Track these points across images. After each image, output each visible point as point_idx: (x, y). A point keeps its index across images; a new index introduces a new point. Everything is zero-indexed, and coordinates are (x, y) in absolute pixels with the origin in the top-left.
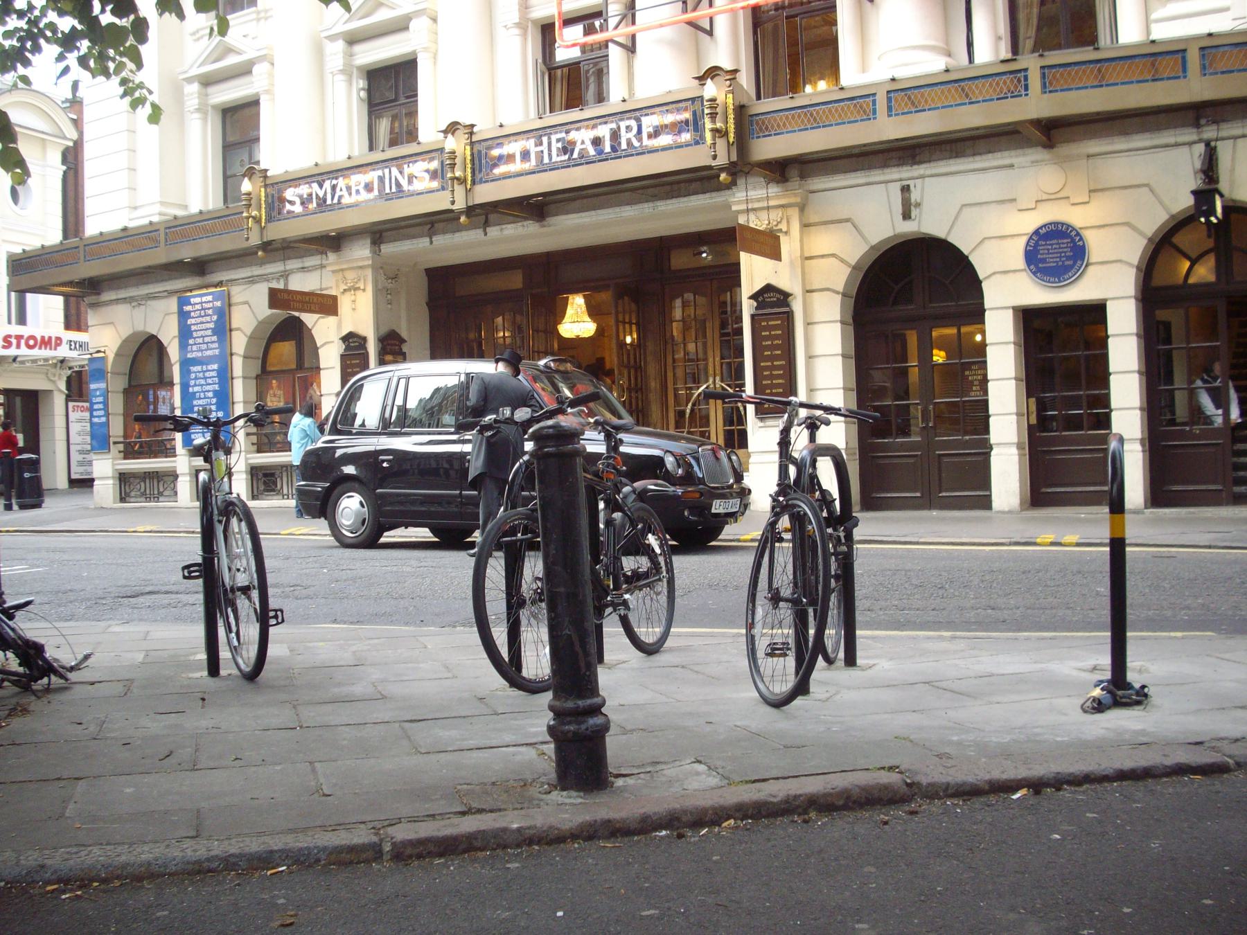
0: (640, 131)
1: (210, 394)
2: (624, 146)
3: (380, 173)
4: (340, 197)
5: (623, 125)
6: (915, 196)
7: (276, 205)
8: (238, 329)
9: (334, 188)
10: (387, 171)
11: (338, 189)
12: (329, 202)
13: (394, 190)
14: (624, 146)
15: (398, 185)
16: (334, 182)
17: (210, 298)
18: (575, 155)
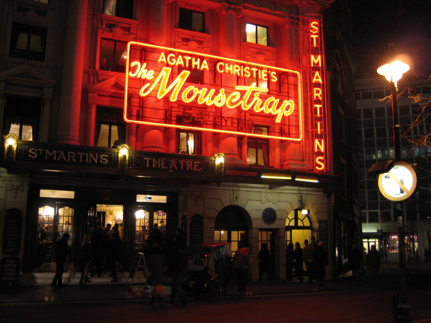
2: (188, 169)
3: (84, 154)
9: (58, 155)
11: (61, 155)
12: (55, 159)
13: (90, 162)
14: (188, 169)
16: (58, 152)
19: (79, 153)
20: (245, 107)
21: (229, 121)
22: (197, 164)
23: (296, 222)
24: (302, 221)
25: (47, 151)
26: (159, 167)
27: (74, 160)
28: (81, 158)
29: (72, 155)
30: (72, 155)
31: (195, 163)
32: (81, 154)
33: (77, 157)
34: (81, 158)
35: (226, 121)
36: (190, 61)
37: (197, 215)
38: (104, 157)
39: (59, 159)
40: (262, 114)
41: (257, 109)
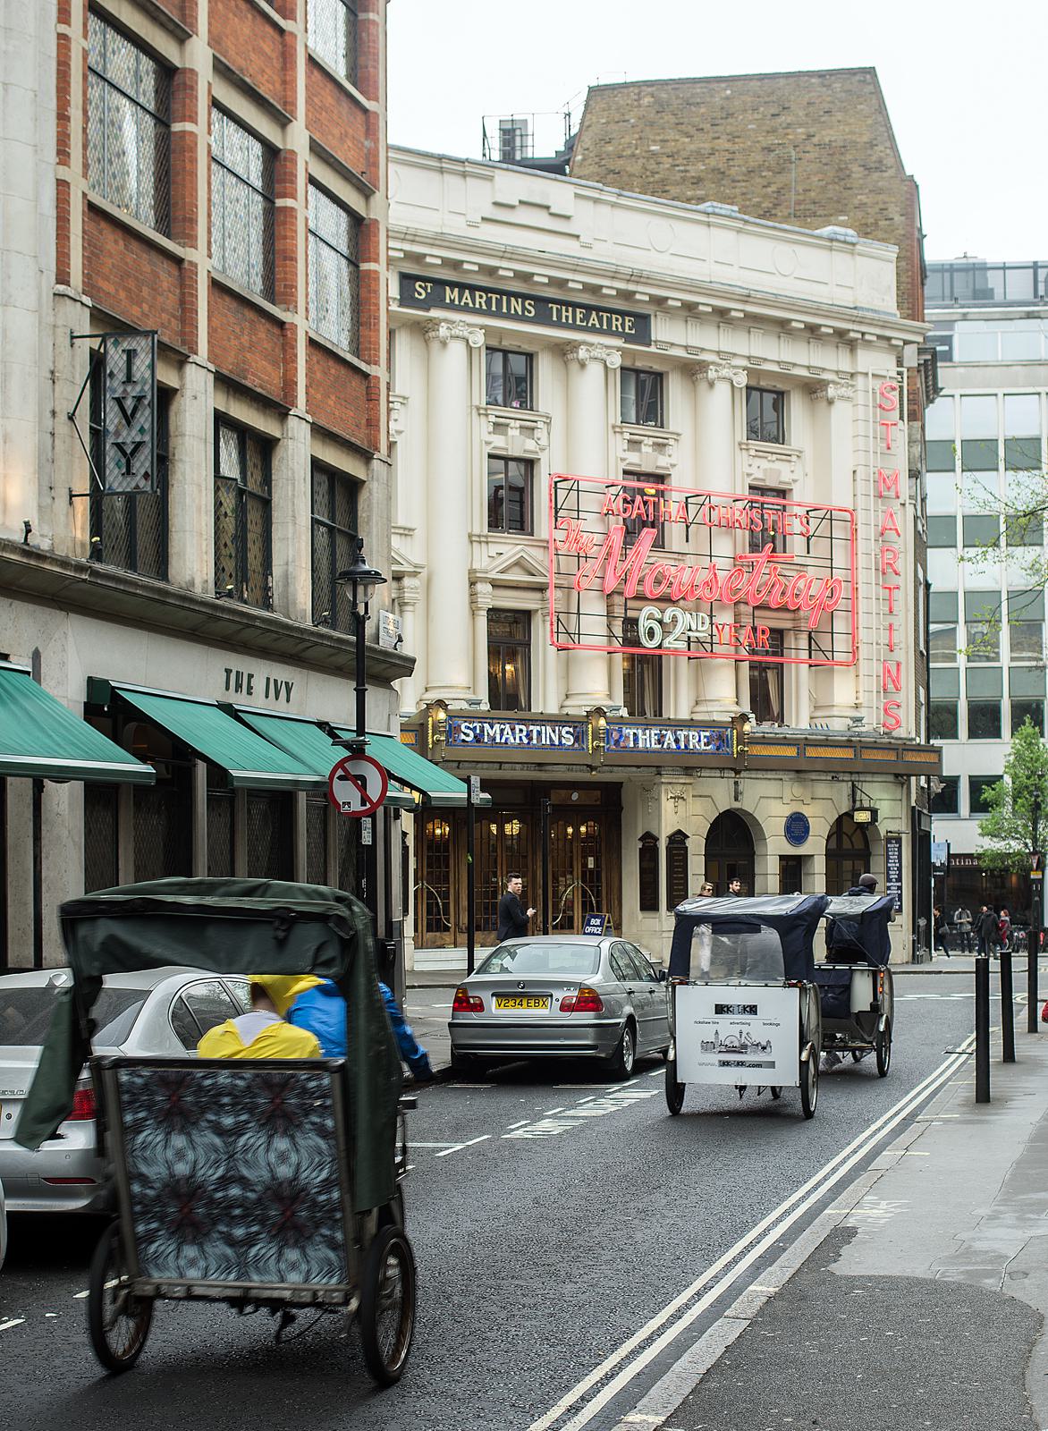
0: (699, 741)
2: (691, 747)
3: (538, 728)
4: (507, 739)
6: (740, 788)
7: (452, 731)
9: (502, 730)
10: (543, 728)
11: (505, 733)
12: (498, 740)
16: (503, 726)
18: (665, 746)
19: (531, 728)
21: (727, 628)
22: (705, 737)
26: (648, 746)
27: (525, 741)
28: (535, 735)
29: (521, 731)
30: (521, 731)
31: (703, 734)
32: (535, 729)
33: (529, 736)
34: (535, 735)
37: (679, 832)
38: (567, 733)
40: (784, 609)
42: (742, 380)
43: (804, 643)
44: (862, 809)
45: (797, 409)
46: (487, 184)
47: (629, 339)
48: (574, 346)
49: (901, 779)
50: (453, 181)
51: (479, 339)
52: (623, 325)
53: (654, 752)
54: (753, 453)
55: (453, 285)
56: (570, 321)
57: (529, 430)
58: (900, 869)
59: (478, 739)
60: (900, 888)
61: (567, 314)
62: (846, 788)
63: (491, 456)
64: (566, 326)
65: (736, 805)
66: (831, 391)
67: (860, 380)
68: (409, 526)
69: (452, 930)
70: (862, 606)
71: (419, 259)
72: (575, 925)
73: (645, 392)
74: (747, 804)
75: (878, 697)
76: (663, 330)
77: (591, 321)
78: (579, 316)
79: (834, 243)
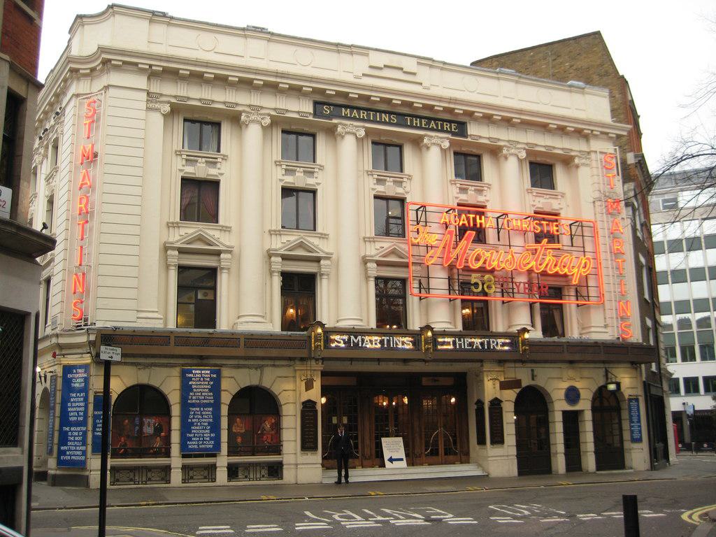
1: (206, 424)
3: (388, 338)
5: (491, 340)
6: (535, 373)
8: (225, 391)
9: (363, 340)
12: (360, 345)
15: (397, 344)
17: (209, 372)
19: (383, 338)
20: (537, 268)
23: (601, 403)
24: (608, 401)
25: (352, 337)
26: (463, 347)
32: (386, 338)
33: (382, 342)
35: (518, 287)
36: (475, 219)
37: (496, 399)
39: (364, 345)
40: (556, 275)
41: (550, 269)
42: (523, 155)
43: (573, 293)
44: (612, 383)
45: (560, 175)
46: (365, 58)
47: (453, 134)
48: (421, 138)
49: (635, 365)
50: (346, 58)
51: (362, 133)
52: (451, 127)
53: (466, 350)
54: (535, 194)
55: (346, 107)
56: (418, 125)
57: (399, 183)
58: (639, 416)
59: (348, 342)
60: (640, 426)
61: (416, 122)
62: (602, 372)
63: (376, 197)
64: (416, 128)
65: (532, 383)
66: (577, 161)
67: (593, 155)
68: (325, 232)
69: (360, 458)
70: (604, 272)
71: (322, 92)
72: (440, 453)
73: (469, 164)
74: (540, 382)
75: (617, 321)
76: (473, 130)
77: (431, 126)
78: (423, 123)
79: (572, 88)
